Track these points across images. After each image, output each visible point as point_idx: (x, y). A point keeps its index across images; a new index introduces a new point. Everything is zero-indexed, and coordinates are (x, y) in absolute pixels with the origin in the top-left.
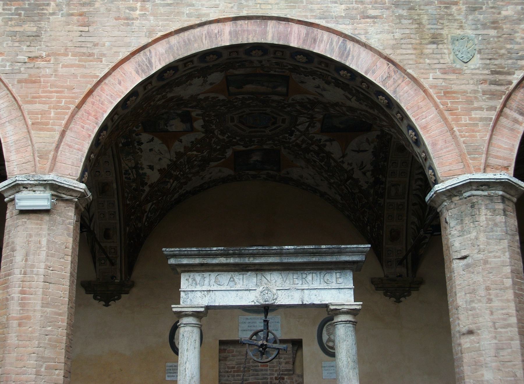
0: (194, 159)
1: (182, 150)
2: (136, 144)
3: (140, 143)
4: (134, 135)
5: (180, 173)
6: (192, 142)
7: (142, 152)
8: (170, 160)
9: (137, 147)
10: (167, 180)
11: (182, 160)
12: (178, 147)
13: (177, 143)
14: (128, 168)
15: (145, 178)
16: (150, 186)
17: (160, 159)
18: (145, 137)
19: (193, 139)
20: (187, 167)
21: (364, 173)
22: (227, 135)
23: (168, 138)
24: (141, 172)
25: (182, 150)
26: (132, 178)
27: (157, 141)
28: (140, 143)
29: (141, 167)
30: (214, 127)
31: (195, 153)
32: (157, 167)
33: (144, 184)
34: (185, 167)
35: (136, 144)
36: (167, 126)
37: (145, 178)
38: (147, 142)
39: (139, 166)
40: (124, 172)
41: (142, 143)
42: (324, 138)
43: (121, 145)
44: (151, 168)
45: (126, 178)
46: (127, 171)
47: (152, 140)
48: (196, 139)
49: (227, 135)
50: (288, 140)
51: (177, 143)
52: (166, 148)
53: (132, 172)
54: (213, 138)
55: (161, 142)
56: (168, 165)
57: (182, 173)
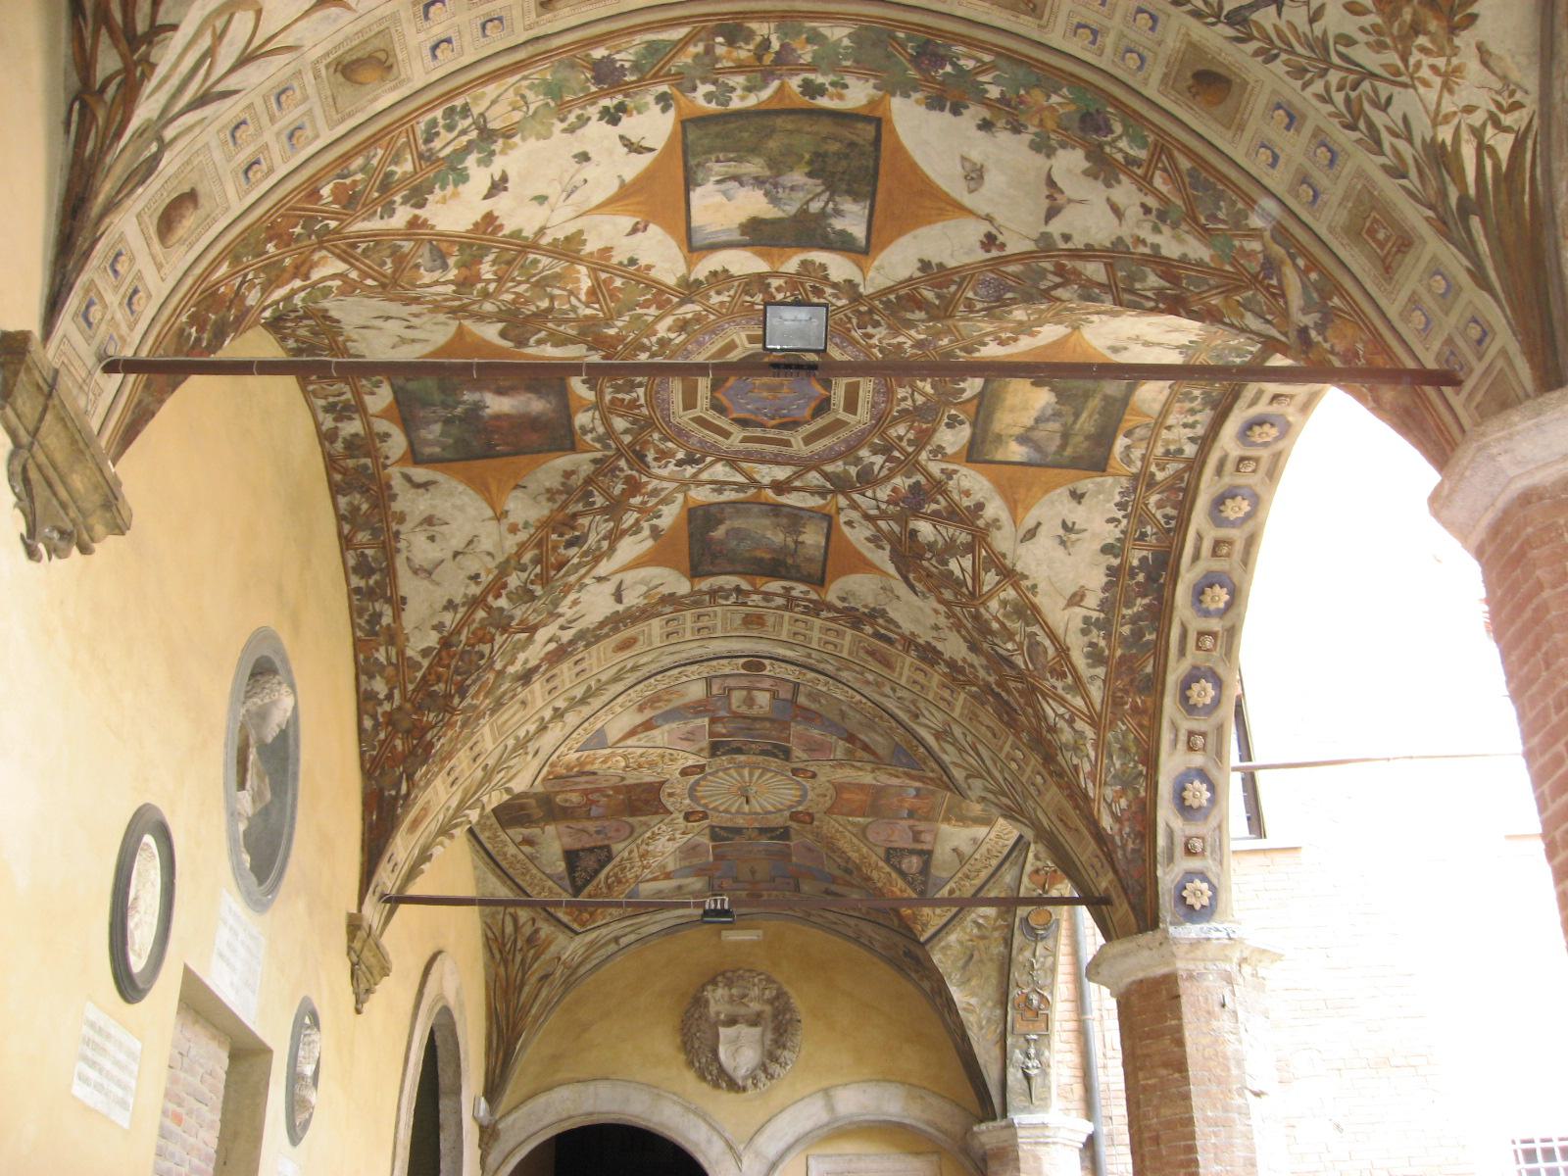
0: (557, 292)
1: (592, 246)
2: (607, 102)
3: (612, 117)
4: (664, 88)
5: (489, 281)
6: (632, 261)
7: (571, 130)
8: (542, 231)
9: (593, 111)
10: (451, 261)
11: (545, 261)
12: (610, 233)
13: (627, 222)
14: (476, 111)
15: (443, 188)
16: (414, 223)
17: (541, 199)
18: (654, 125)
19: (643, 262)
20: (521, 289)
21: (550, 640)
22: (672, 336)
23: (660, 195)
24: (471, 161)
25: (592, 246)
26: (437, 144)
27: (635, 166)
28: (612, 117)
29: (492, 153)
30: (715, 299)
31: (586, 283)
32: (501, 205)
33: (418, 196)
34: (519, 283)
35: (607, 102)
36: (718, 182)
37: (443, 188)
38: (622, 137)
39: (498, 146)
40: (458, 102)
41: (614, 121)
42: (669, 515)
43: (598, 53)
44: (498, 186)
45: (434, 123)
46: (466, 111)
47: (634, 147)
48: (649, 268)
49: (672, 336)
50: (653, 464)
51: (627, 222)
52: (598, 198)
53: (464, 132)
54: (658, 308)
55: (629, 175)
56: (517, 234)
57: (492, 287)
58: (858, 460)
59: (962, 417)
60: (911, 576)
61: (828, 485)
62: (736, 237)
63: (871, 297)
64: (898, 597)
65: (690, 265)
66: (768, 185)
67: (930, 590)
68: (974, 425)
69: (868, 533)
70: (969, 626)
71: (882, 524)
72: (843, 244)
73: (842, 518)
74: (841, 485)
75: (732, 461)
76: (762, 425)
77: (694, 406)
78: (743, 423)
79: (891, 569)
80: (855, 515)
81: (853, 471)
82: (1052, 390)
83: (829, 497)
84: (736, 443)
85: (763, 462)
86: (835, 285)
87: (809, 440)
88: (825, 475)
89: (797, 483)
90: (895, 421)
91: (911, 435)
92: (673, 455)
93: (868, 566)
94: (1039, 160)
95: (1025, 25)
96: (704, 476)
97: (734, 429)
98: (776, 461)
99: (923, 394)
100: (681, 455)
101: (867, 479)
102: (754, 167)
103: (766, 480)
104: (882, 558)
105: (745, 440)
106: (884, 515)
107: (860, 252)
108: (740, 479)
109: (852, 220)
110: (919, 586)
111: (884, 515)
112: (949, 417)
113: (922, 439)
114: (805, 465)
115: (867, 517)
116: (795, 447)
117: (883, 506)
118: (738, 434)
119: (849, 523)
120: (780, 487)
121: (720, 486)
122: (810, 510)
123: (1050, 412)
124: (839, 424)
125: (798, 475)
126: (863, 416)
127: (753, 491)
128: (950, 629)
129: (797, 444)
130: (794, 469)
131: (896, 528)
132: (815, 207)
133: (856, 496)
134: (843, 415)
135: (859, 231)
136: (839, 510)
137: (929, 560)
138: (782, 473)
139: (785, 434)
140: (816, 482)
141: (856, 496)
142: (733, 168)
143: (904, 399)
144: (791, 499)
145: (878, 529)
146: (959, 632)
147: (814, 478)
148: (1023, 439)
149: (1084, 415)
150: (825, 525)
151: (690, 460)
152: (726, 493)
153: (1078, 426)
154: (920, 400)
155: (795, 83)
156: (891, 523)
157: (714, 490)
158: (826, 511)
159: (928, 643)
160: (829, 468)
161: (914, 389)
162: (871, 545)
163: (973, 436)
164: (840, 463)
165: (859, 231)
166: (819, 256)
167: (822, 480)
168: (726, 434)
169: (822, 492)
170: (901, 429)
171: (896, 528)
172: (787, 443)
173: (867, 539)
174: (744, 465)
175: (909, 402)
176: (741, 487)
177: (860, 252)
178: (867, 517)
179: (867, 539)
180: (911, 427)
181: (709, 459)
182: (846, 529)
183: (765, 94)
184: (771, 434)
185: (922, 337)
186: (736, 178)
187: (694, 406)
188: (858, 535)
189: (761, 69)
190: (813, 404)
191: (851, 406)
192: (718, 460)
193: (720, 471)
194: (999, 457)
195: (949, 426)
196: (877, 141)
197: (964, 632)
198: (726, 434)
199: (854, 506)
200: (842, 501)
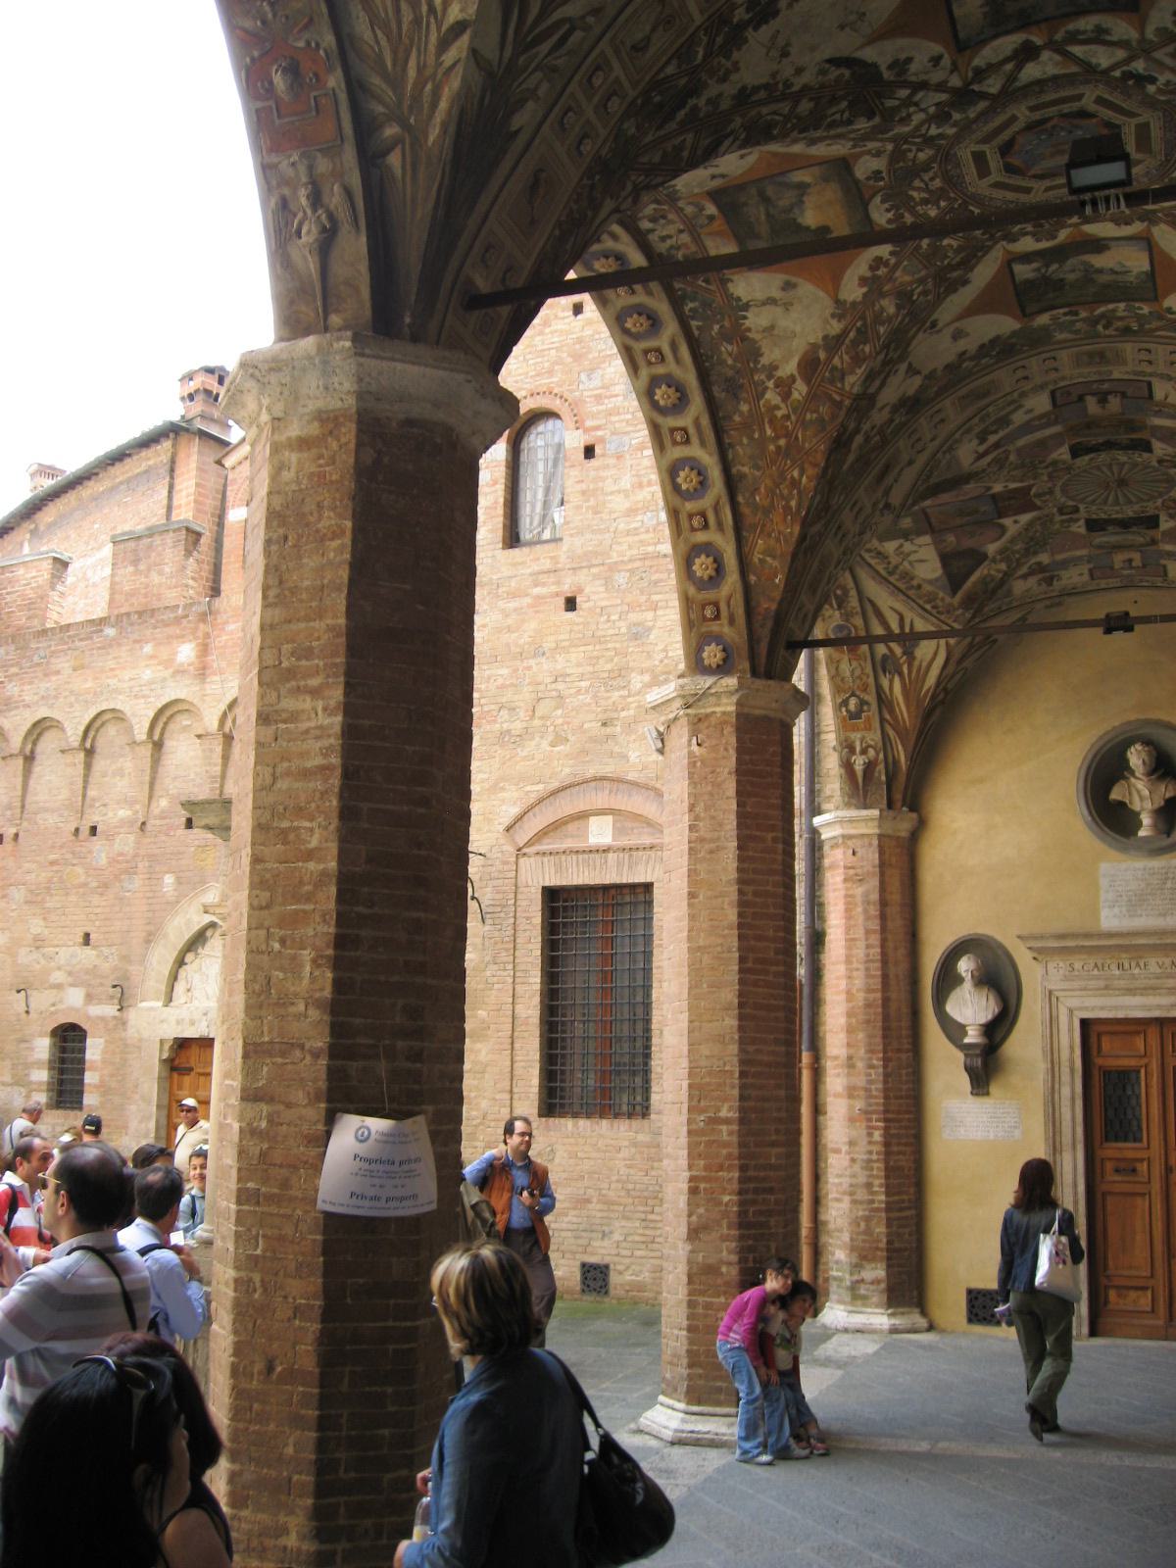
58: (954, 125)
59: (871, 182)
60: (847, 73)
61: (976, 87)
62: (1113, 243)
63: (996, 243)
64: (842, 27)
65: (1149, 230)
66: (1089, 274)
67: (822, 86)
68: (856, 182)
69: (913, 67)
70: (765, 110)
71: (904, 93)
72: (1026, 258)
73: (946, 62)
74: (964, 96)
75: (1090, 72)
76: (1064, 116)
77: (1138, 126)
78: (1083, 114)
79: (869, 54)
80: (936, 77)
81: (956, 116)
82: (807, 228)
83: (970, 74)
84: (1088, 93)
85: (1055, 78)
86: (1026, 234)
87: (1014, 119)
88: (983, 96)
89: (1009, 67)
90: (932, 159)
91: (911, 155)
92: (1159, 90)
93: (895, 28)
94: (926, 372)
95: (960, 393)
96: (1121, 54)
97: (1092, 107)
98: (1040, 84)
99: (918, 189)
100: (1151, 89)
101: (942, 116)
102: (1104, 278)
103: (1046, 55)
104: (880, 55)
105: (1079, 97)
106: (908, 102)
107: (1011, 260)
108: (1077, 50)
109: (1023, 272)
110: (834, 73)
111: (908, 102)
112: (883, 179)
113: (897, 156)
114: (1010, 93)
115: (924, 85)
116: (1023, 108)
117: (912, 109)
118: (1088, 102)
119: (936, 60)
120: (1028, 52)
121: (1099, 37)
122: (983, 43)
123: (796, 210)
124: (986, 140)
125: (1012, 78)
126: (965, 153)
127: (1058, 37)
128: (774, 75)
129: (1022, 112)
130: (1018, 84)
131: (890, 103)
132: (1055, 266)
133: (944, 97)
134: (985, 148)
135: (1018, 268)
136: (955, 68)
137: (843, 112)
138: (1031, 71)
139: (1037, 115)
140: (990, 81)
141: (944, 97)
142: (1120, 278)
143: (932, 179)
144: (1009, 43)
145: (905, 84)
146: (766, 86)
147: (993, 85)
148: (802, 187)
149: (763, 217)
150: (962, 35)
151: (1143, 80)
152: (1090, 27)
153: (762, 209)
154: (917, 183)
155: (1083, 314)
156: (897, 103)
157: (1107, 31)
158: (968, 52)
159: (776, 13)
160: (982, 105)
161: (927, 189)
162: (903, 56)
163: (851, 173)
164: (972, 116)
165: (1018, 268)
166: (1045, 245)
167: (985, 89)
168: (1100, 101)
169: (980, 74)
170: (922, 156)
171: (890, 103)
172: (1032, 109)
173: (909, 60)
174: (1074, 69)
175: (926, 178)
176: (1073, 38)
177: (1011, 260)
178: (924, 85)
179: (909, 60)
180: (914, 160)
181: (1117, 74)
182: (937, 49)
183: (1102, 309)
184: (1052, 111)
185: (945, 242)
186: (1116, 273)
187: (1138, 126)
188: (922, 52)
189: (1108, 320)
190: (1016, 147)
191: (980, 159)
192: (1106, 72)
193: (1103, 58)
194: (816, 170)
195: (879, 172)
196: (1023, 310)
197: (762, 94)
198: (1100, 101)
199: (941, 87)
200: (955, 81)
